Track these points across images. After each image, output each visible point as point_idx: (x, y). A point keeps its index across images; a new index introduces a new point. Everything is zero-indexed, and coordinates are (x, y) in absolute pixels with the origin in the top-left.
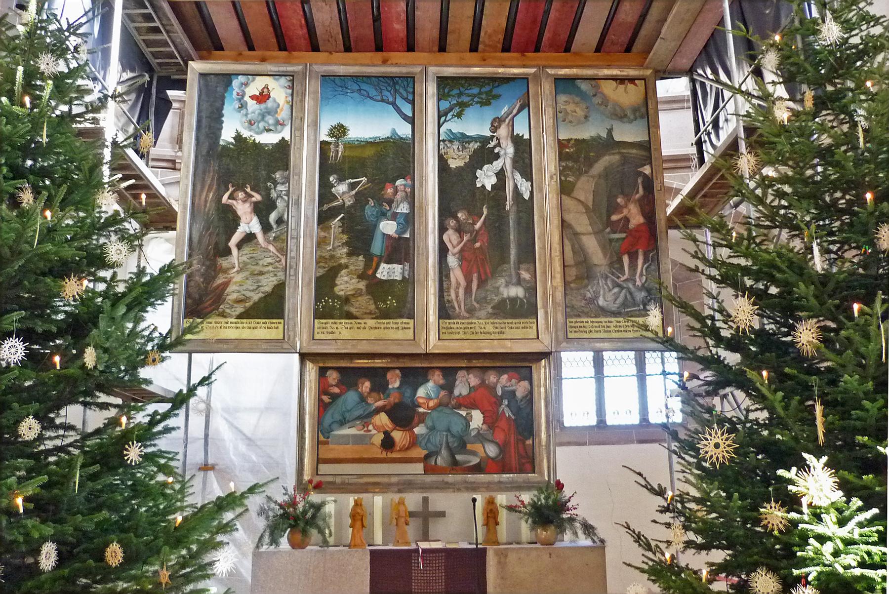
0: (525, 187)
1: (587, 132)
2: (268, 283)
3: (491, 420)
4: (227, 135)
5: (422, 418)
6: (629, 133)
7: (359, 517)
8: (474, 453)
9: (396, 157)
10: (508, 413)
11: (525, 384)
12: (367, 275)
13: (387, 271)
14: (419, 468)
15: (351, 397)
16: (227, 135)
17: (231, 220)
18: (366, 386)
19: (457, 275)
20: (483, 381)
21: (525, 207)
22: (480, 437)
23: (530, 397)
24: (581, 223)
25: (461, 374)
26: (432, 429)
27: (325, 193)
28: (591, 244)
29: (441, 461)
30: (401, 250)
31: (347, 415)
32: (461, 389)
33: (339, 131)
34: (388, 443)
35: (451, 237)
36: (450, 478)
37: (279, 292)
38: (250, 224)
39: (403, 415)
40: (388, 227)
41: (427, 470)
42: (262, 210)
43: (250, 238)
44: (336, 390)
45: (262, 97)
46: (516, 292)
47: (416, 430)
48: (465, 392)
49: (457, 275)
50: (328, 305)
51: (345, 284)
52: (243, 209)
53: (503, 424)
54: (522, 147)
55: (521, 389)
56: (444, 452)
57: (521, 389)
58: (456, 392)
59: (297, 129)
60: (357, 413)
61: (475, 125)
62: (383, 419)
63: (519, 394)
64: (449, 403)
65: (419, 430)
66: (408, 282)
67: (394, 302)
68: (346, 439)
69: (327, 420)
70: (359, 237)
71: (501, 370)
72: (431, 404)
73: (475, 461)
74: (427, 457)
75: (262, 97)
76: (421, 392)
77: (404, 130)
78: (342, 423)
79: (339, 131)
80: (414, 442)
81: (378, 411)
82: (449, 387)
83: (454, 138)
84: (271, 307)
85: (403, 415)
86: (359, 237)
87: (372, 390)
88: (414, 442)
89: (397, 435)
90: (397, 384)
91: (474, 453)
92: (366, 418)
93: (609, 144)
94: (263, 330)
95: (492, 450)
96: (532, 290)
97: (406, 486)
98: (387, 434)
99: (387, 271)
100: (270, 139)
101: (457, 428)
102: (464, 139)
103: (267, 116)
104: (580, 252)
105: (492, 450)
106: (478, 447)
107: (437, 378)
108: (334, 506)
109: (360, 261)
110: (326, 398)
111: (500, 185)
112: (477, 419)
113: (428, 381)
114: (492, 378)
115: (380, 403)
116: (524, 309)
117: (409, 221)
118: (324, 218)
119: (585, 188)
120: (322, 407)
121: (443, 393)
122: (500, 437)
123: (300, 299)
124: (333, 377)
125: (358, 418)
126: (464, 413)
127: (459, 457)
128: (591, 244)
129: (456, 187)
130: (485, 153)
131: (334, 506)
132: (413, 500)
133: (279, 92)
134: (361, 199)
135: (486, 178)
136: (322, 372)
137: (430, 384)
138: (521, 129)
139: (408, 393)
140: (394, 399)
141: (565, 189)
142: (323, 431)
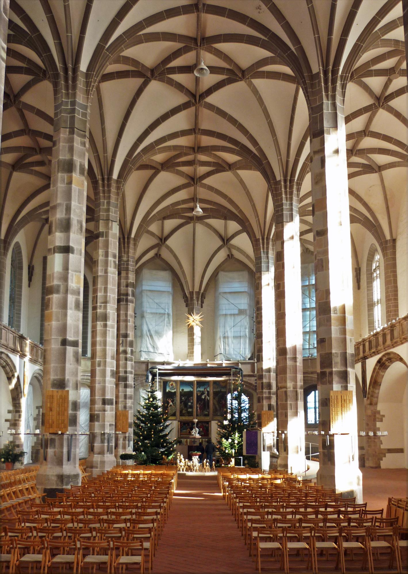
0: (208, 398)
1: (218, 390)
2: (174, 411)
4: (167, 391)
6: (223, 390)
7: (186, 442)
9: (190, 394)
12: (187, 410)
13: (190, 410)
16: (167, 391)
17: (168, 403)
19: (199, 410)
21: (208, 401)
24: (216, 403)
27: (181, 399)
28: (217, 406)
30: (191, 407)
33: (183, 390)
35: (198, 405)
37: (175, 412)
38: (171, 403)
40: (190, 404)
42: (172, 401)
43: (171, 405)
45: (172, 385)
46: (207, 413)
49: (199, 410)
50: (182, 414)
51: (184, 412)
52: (170, 401)
54: (208, 392)
55: (207, 425)
59: (177, 390)
61: (202, 389)
66: (192, 411)
67: (190, 414)
70: (186, 405)
75: (172, 385)
77: (192, 390)
79: (183, 390)
83: (199, 391)
84: (174, 415)
86: (186, 405)
92: (186, 429)
93: (221, 392)
94: (173, 418)
96: (209, 412)
99: (190, 410)
100: (173, 391)
102: (200, 391)
103: (172, 388)
104: (216, 407)
108: (183, 440)
109: (186, 409)
111: (205, 398)
116: (208, 415)
117: (192, 403)
118: (181, 402)
119: (217, 398)
120: (181, 427)
123: (178, 414)
128: (217, 406)
129: (199, 398)
130: (203, 393)
131: (183, 440)
133: (174, 384)
134: (186, 400)
135: (203, 397)
136: (181, 423)
138: (208, 390)
141: (214, 398)
142: (181, 430)
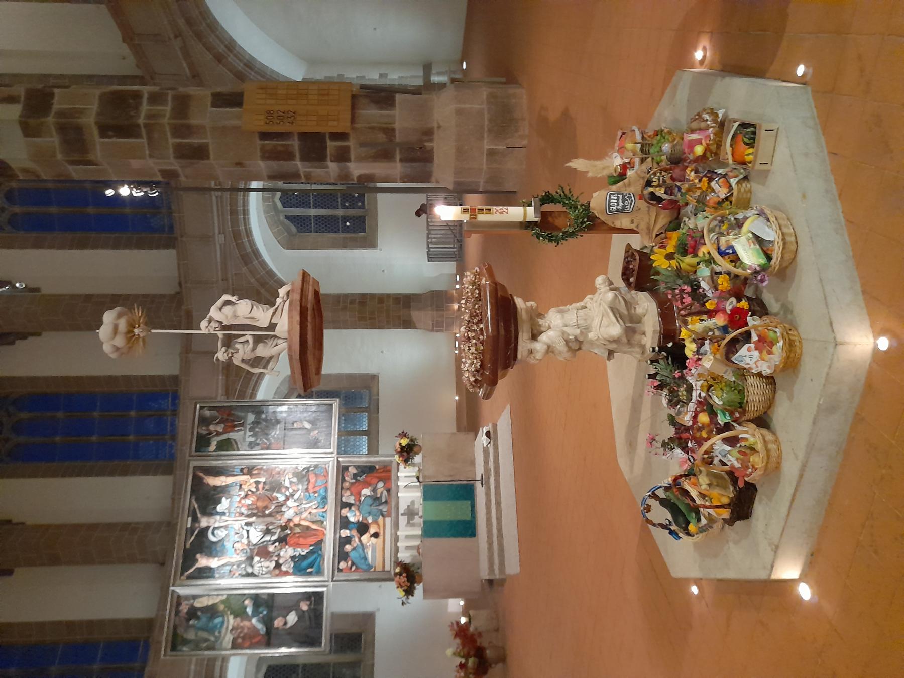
3: (367, 484)
5: (365, 518)
8: (382, 493)
10: (363, 477)
11: (350, 468)
14: (388, 520)
15: (352, 555)
18: (348, 548)
20: (348, 489)
22: (374, 490)
23: (357, 467)
25: (344, 500)
26: (370, 513)
29: (384, 508)
31: (362, 556)
32: (351, 500)
34: (376, 535)
36: (393, 504)
39: (362, 528)
41: (389, 515)
44: (350, 563)
47: (370, 521)
48: (353, 498)
53: (369, 479)
56: (381, 507)
57: (352, 470)
58: (353, 502)
60: (361, 550)
62: (365, 538)
63: (355, 471)
64: (359, 505)
65: (370, 520)
68: (373, 557)
69: (364, 567)
71: (343, 480)
72: (358, 514)
73: (385, 493)
74: (383, 516)
76: (352, 519)
78: (365, 559)
80: (375, 522)
81: (360, 541)
82: (349, 505)
85: (362, 528)
87: (350, 544)
88: (375, 522)
89: (372, 530)
90: (348, 531)
91: (382, 493)
95: (381, 484)
97: (396, 526)
98: (371, 536)
101: (370, 501)
105: (381, 484)
106: (379, 491)
107: (345, 512)
110: (354, 568)
112: (366, 492)
113: (346, 517)
114: (346, 485)
115: (357, 540)
121: (353, 508)
122: (375, 480)
124: (342, 565)
125: (363, 550)
126: (363, 498)
127: (383, 500)
132: (403, 520)
137: (348, 515)
139: (351, 526)
140: (354, 533)
